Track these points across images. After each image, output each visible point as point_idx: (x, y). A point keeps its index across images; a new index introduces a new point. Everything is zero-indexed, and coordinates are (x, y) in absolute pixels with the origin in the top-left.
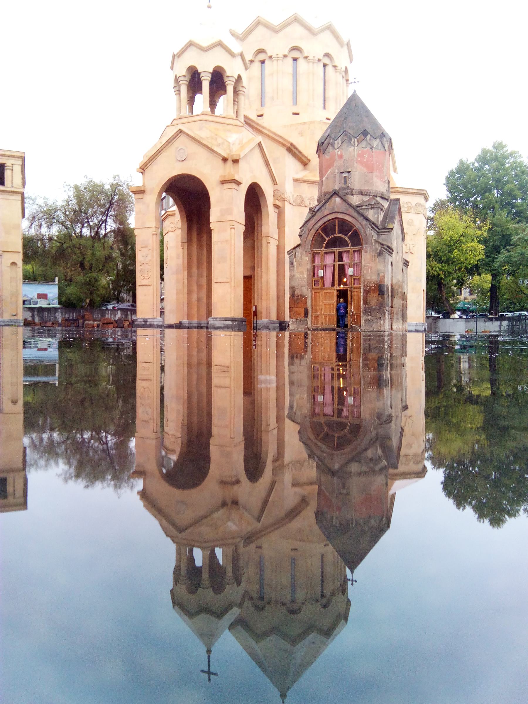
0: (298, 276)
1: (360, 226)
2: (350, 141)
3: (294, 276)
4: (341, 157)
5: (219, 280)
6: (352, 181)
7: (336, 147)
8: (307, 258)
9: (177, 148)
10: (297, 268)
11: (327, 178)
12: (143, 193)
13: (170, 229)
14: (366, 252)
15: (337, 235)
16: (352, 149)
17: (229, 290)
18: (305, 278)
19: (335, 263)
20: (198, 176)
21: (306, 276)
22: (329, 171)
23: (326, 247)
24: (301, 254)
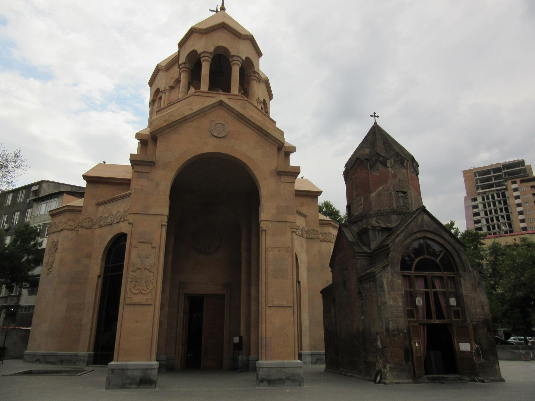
1: (452, 249)
2: (402, 163)
3: (385, 303)
4: (395, 176)
5: (276, 303)
6: (410, 202)
7: (388, 165)
8: (400, 281)
9: (213, 121)
10: (389, 293)
11: (379, 195)
12: (151, 166)
13: (67, 227)
14: (465, 280)
15: (427, 257)
16: (404, 171)
17: (292, 319)
18: (399, 306)
19: (429, 290)
20: (243, 160)
21: (400, 304)
22: (381, 188)
23: (416, 269)
24: (392, 275)
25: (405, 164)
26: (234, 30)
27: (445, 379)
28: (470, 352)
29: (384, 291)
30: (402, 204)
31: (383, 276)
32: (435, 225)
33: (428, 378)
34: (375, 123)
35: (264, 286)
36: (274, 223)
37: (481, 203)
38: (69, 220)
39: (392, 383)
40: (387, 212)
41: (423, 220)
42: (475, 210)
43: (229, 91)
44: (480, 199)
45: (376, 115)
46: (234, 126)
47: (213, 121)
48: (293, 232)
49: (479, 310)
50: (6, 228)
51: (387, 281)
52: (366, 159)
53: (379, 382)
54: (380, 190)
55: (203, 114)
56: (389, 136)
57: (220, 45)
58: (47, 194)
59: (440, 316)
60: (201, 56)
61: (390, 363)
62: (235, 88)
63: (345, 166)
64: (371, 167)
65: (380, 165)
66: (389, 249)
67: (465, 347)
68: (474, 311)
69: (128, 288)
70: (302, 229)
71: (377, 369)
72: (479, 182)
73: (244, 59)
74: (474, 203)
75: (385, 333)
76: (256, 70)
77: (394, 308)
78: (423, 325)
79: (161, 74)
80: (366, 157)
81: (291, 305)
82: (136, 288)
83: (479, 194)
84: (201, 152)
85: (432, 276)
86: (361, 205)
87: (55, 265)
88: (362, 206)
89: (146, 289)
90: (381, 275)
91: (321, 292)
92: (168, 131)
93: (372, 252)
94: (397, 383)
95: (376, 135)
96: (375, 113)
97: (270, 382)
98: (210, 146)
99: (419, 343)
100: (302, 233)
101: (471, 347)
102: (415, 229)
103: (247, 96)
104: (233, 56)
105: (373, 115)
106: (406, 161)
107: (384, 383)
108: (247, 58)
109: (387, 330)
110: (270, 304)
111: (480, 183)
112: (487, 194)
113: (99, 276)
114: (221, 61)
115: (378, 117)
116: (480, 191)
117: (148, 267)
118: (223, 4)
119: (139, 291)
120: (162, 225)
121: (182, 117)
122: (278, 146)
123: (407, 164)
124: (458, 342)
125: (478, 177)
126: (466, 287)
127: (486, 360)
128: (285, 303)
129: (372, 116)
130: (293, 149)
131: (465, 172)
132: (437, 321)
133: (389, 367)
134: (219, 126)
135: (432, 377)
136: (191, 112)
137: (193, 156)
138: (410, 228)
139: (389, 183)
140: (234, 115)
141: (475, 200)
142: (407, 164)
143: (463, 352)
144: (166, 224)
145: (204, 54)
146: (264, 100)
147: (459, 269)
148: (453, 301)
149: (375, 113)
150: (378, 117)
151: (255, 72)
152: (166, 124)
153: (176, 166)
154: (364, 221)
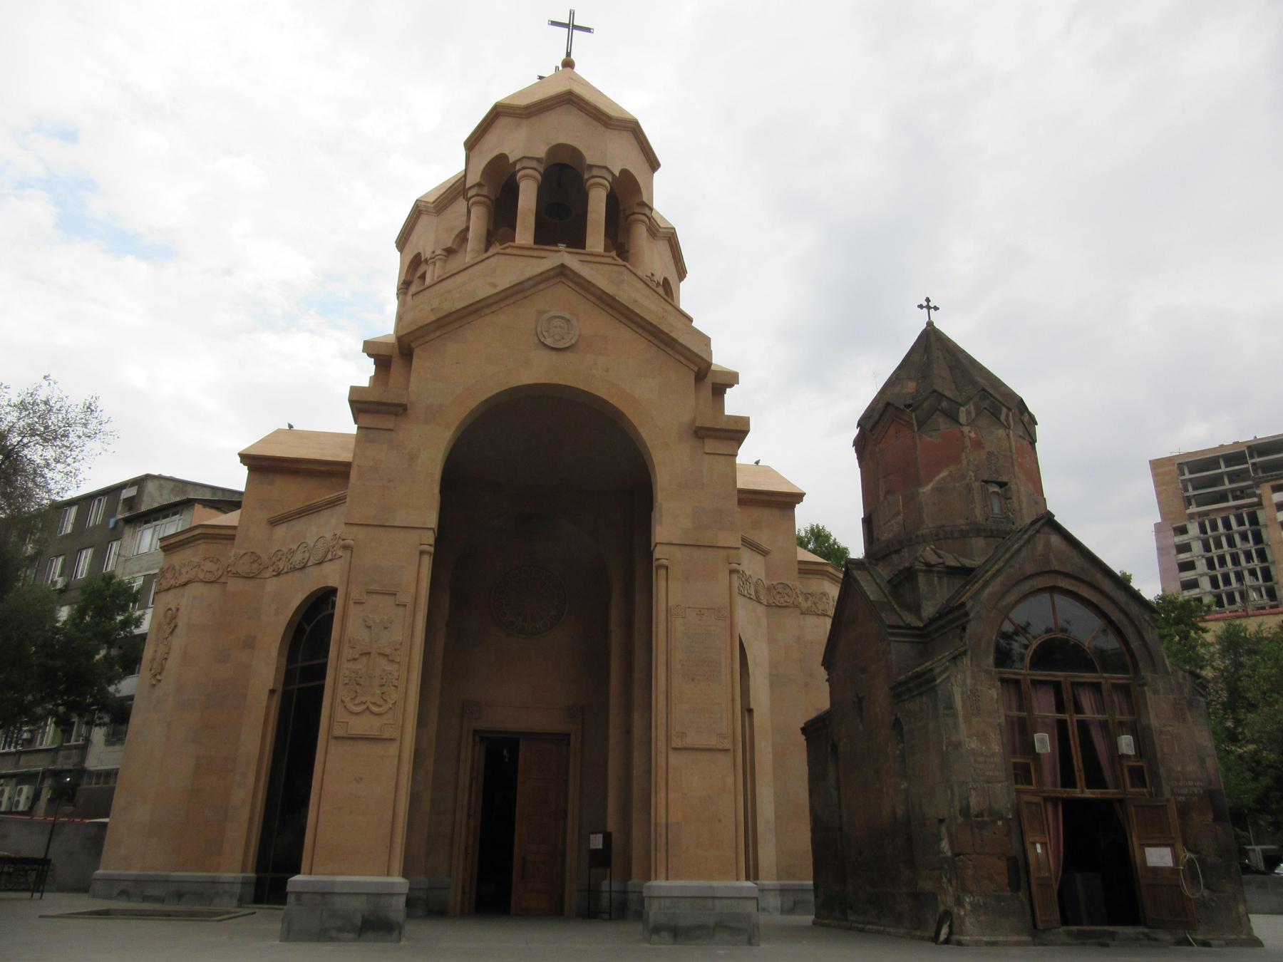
0: (973, 746)
1: (1122, 617)
2: (995, 414)
3: (958, 745)
4: (978, 445)
5: (693, 739)
6: (1016, 505)
7: (963, 418)
8: (994, 693)
9: (544, 312)
11: (939, 490)
12: (396, 415)
13: (201, 576)
14: (1156, 692)
16: (1001, 432)
18: (994, 754)
21: (997, 748)
25: (1003, 418)
26: (595, 108)
27: (1112, 935)
28: (1174, 871)
29: (955, 715)
30: (996, 510)
31: (953, 679)
32: (1077, 559)
33: (1069, 933)
34: (930, 324)
35: (662, 698)
36: (687, 550)
37: (1199, 538)
38: (205, 559)
39: (977, 943)
40: (961, 531)
41: (1048, 545)
42: (1184, 557)
43: (584, 247)
44: (1194, 529)
45: (931, 304)
46: (592, 322)
47: (544, 312)
48: (732, 572)
49: (1192, 768)
50: (59, 586)
51: (963, 693)
52: (908, 406)
53: (947, 941)
54: (944, 479)
55: (521, 295)
56: (963, 351)
57: (562, 140)
58: (156, 505)
59: (1095, 780)
60: (518, 167)
61: (971, 893)
62: (596, 239)
63: (859, 425)
64: (921, 424)
65: (940, 420)
66: (967, 614)
67: (1159, 857)
68: (1179, 768)
69: (338, 701)
70: (756, 584)
71: (941, 908)
72: (1190, 488)
73: (617, 174)
74: (1179, 539)
75: (960, 820)
76: (645, 199)
77: (981, 759)
78: (1055, 801)
79: (424, 221)
80: (908, 402)
81: (728, 746)
82: (358, 701)
83: (1191, 516)
84: (514, 382)
85: (1073, 684)
86: (898, 513)
87: (172, 664)
88: (900, 518)
89: (380, 702)
90: (948, 677)
91: (804, 730)
92: (438, 333)
93: (926, 626)
94: (992, 944)
95: (932, 350)
96: (928, 300)
97: (678, 933)
98: (536, 370)
99: (1044, 845)
100: (756, 592)
101: (1175, 857)
102: (1029, 570)
103: (625, 259)
104: (591, 167)
105: (925, 304)
106: (1004, 410)
107: (960, 943)
108: (625, 173)
109: (965, 812)
110: (676, 742)
111: (1194, 489)
112: (1212, 517)
113: (272, 692)
114: (564, 179)
115: (936, 308)
116: (1193, 509)
117: (387, 651)
118: (568, 54)
119: (364, 707)
120: (422, 553)
121: (471, 301)
122: (696, 369)
123: (1007, 416)
124: (1142, 846)
125: (1187, 476)
126: (1158, 709)
127: (1212, 890)
128: (713, 742)
129: (921, 307)
130: (731, 379)
131: (1156, 465)
132: (1089, 794)
133: (971, 903)
134: (558, 322)
135: (1079, 931)
136: (492, 291)
137: (495, 391)
138: (1017, 566)
139: (965, 462)
140: (592, 298)
141: (1182, 530)
142: (1007, 416)
143: (1156, 870)
144: (432, 549)
145: (525, 163)
146: (666, 280)
147: (1141, 665)
148: (1126, 744)
149: (928, 300)
150: (936, 308)
151: (643, 205)
152: (433, 318)
153: (456, 416)
154: (905, 552)
